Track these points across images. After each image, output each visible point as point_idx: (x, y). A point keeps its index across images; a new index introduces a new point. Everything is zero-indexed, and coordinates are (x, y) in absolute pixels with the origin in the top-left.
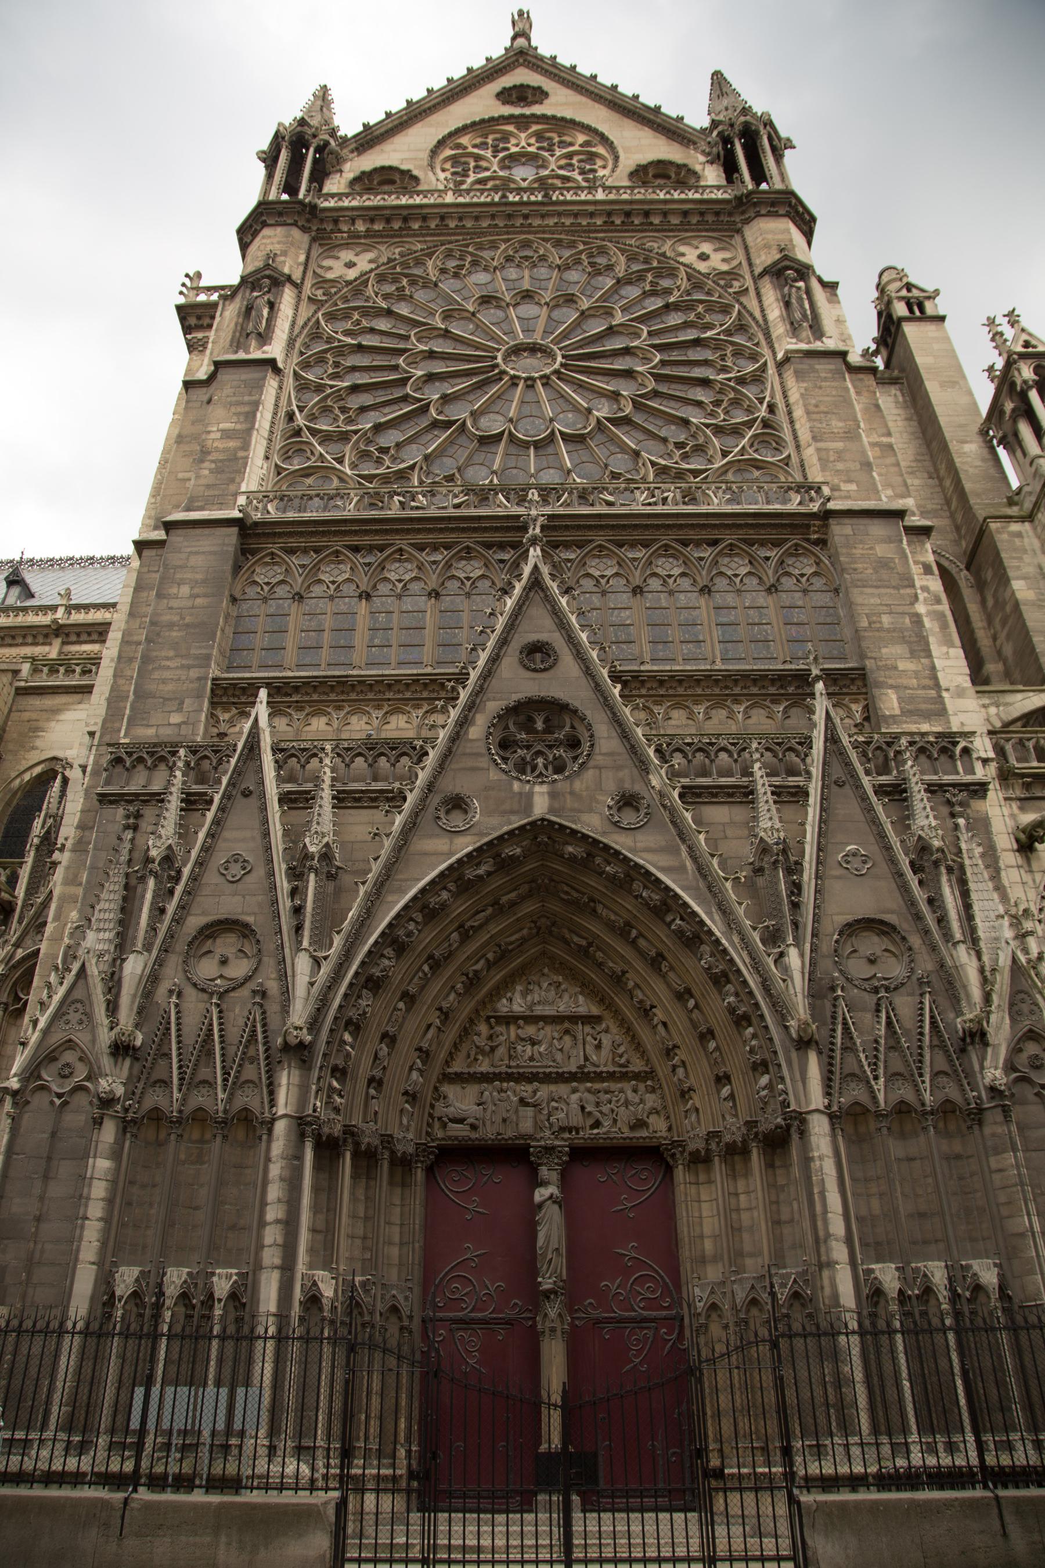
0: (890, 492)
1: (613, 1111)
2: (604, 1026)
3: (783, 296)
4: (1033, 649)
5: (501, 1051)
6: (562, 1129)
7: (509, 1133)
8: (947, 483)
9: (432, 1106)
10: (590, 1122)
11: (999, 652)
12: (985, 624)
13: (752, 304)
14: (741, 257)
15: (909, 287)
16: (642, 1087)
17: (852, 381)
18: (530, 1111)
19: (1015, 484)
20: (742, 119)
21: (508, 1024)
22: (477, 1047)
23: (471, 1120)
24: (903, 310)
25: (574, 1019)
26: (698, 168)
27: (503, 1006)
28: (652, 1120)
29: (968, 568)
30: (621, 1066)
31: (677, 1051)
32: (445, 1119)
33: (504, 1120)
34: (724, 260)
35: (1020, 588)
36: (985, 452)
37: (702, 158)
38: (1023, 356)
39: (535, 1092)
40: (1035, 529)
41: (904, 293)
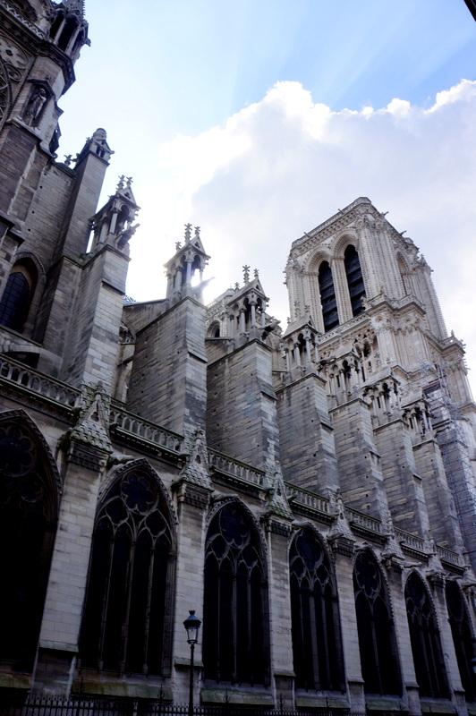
0: (16, 213)
3: (32, 96)
4: (46, 325)
8: (62, 232)
11: (36, 320)
12: (38, 304)
13: (15, 89)
14: (27, 67)
15: (104, 142)
17: (36, 155)
19: (88, 251)
20: (74, 14)
24: (97, 150)
26: (39, 16)
29: (47, 275)
34: (18, 62)
35: (58, 295)
36: (85, 230)
37: (44, 14)
38: (121, 198)
40: (82, 273)
41: (100, 143)
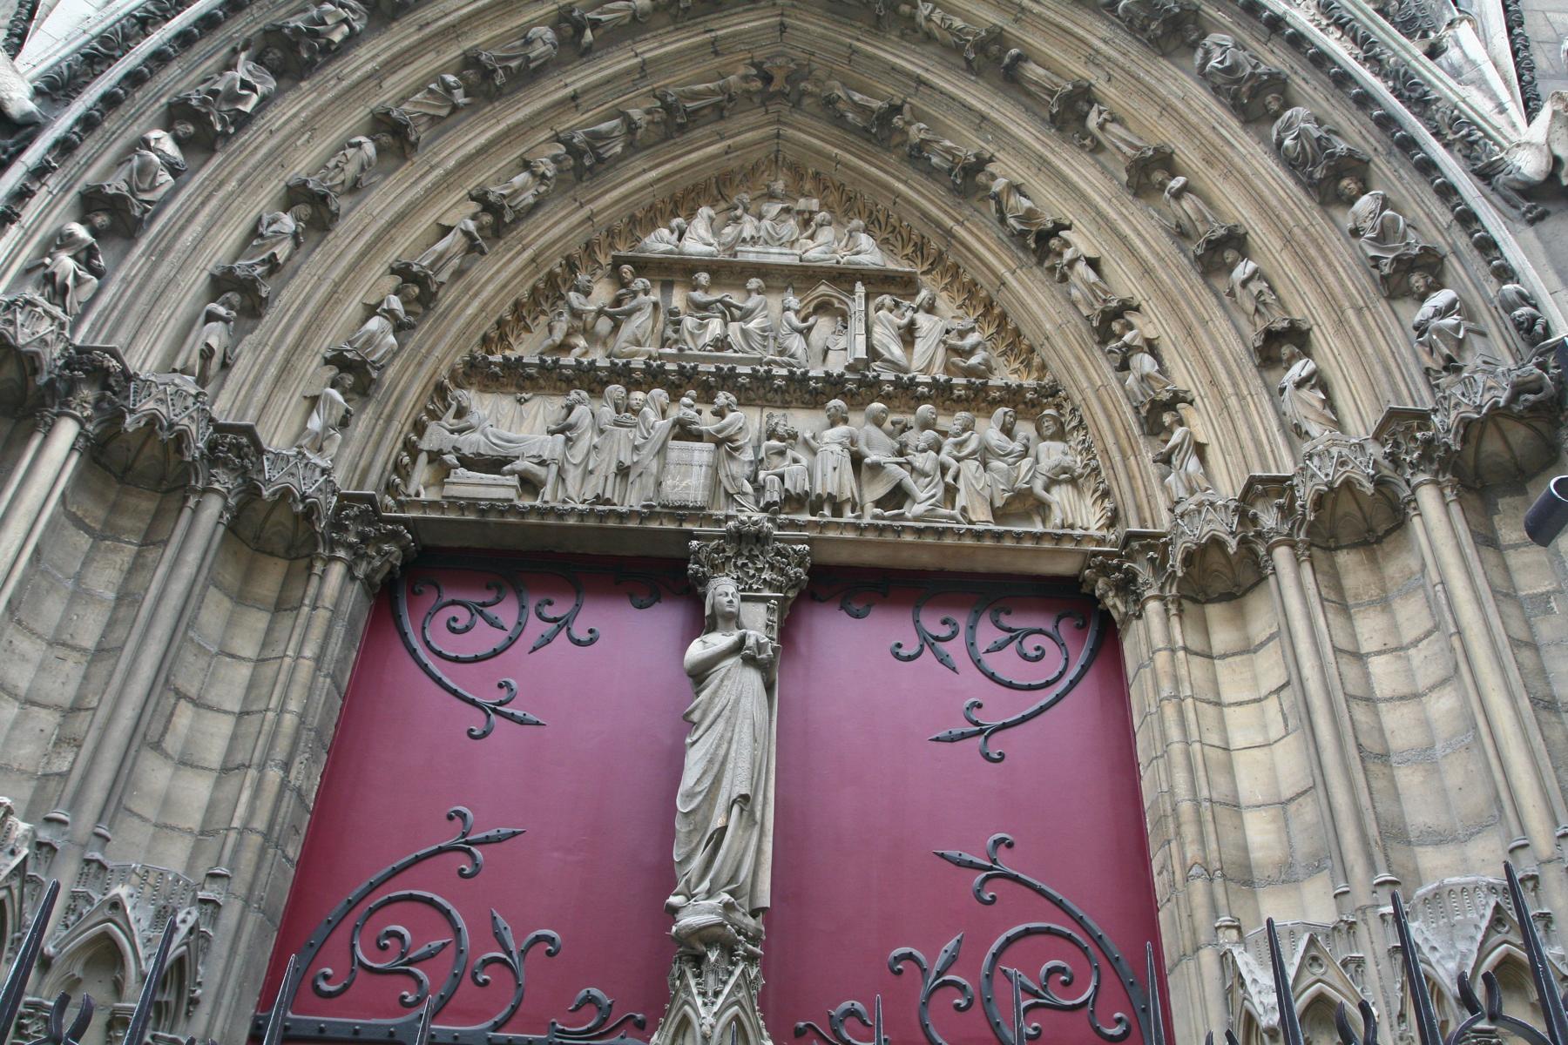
1: (944, 469)
2: (924, 293)
5: (640, 323)
6: (795, 501)
7: (634, 500)
9: (419, 428)
10: (880, 490)
16: (1025, 429)
18: (701, 453)
21: (667, 286)
22: (576, 314)
23: (520, 465)
25: (844, 277)
27: (659, 242)
28: (1060, 497)
30: (969, 372)
31: (1133, 318)
32: (451, 458)
33: (623, 472)
39: (720, 414)
